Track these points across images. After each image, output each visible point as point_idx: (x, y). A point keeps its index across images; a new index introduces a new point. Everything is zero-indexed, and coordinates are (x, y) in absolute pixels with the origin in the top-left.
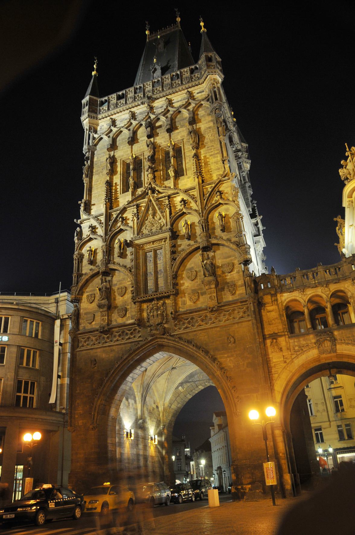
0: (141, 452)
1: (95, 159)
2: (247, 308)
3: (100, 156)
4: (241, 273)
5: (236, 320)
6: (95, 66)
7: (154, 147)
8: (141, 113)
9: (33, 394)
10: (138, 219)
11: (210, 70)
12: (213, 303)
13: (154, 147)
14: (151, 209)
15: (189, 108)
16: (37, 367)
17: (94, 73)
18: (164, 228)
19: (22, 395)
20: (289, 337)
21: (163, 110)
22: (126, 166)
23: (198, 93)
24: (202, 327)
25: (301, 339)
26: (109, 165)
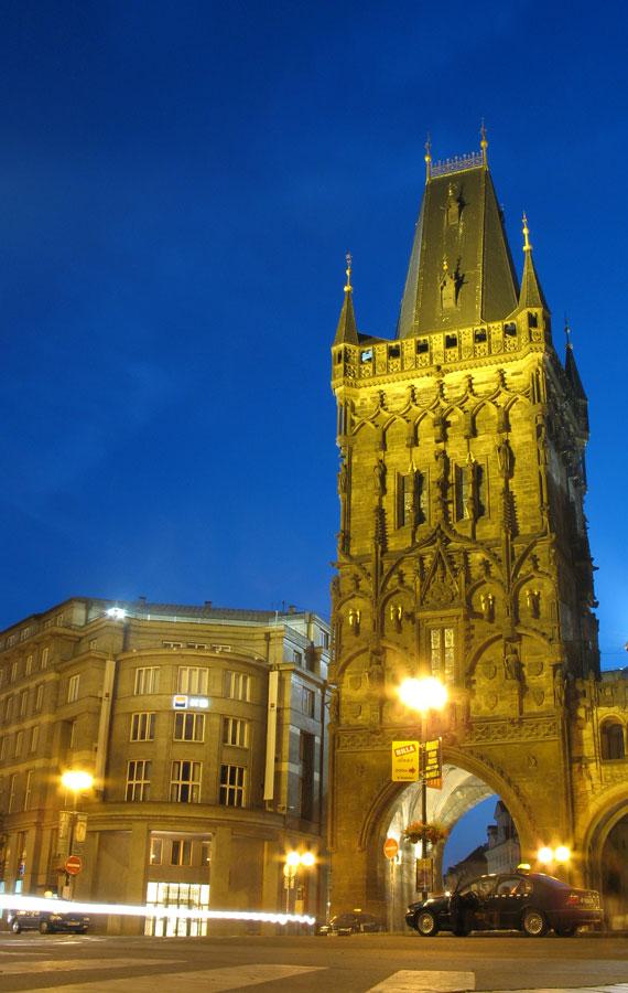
0: (405, 880)
1: (355, 460)
2: (554, 724)
3: (363, 455)
4: (551, 678)
5: (540, 738)
6: (348, 272)
7: (443, 456)
8: (426, 391)
9: (240, 784)
10: (422, 580)
11: (533, 346)
12: (515, 713)
13: (443, 456)
14: (439, 568)
15: (497, 400)
16: (246, 745)
17: (346, 289)
18: (456, 601)
19: (228, 786)
20: (601, 764)
21: (460, 395)
22: (401, 480)
23: (514, 374)
24: (499, 741)
25: (615, 767)
26: (378, 480)
